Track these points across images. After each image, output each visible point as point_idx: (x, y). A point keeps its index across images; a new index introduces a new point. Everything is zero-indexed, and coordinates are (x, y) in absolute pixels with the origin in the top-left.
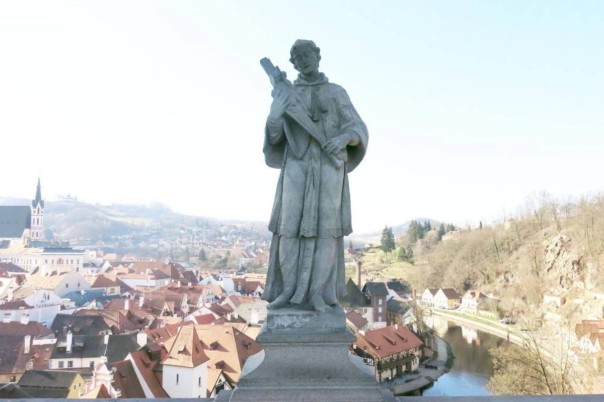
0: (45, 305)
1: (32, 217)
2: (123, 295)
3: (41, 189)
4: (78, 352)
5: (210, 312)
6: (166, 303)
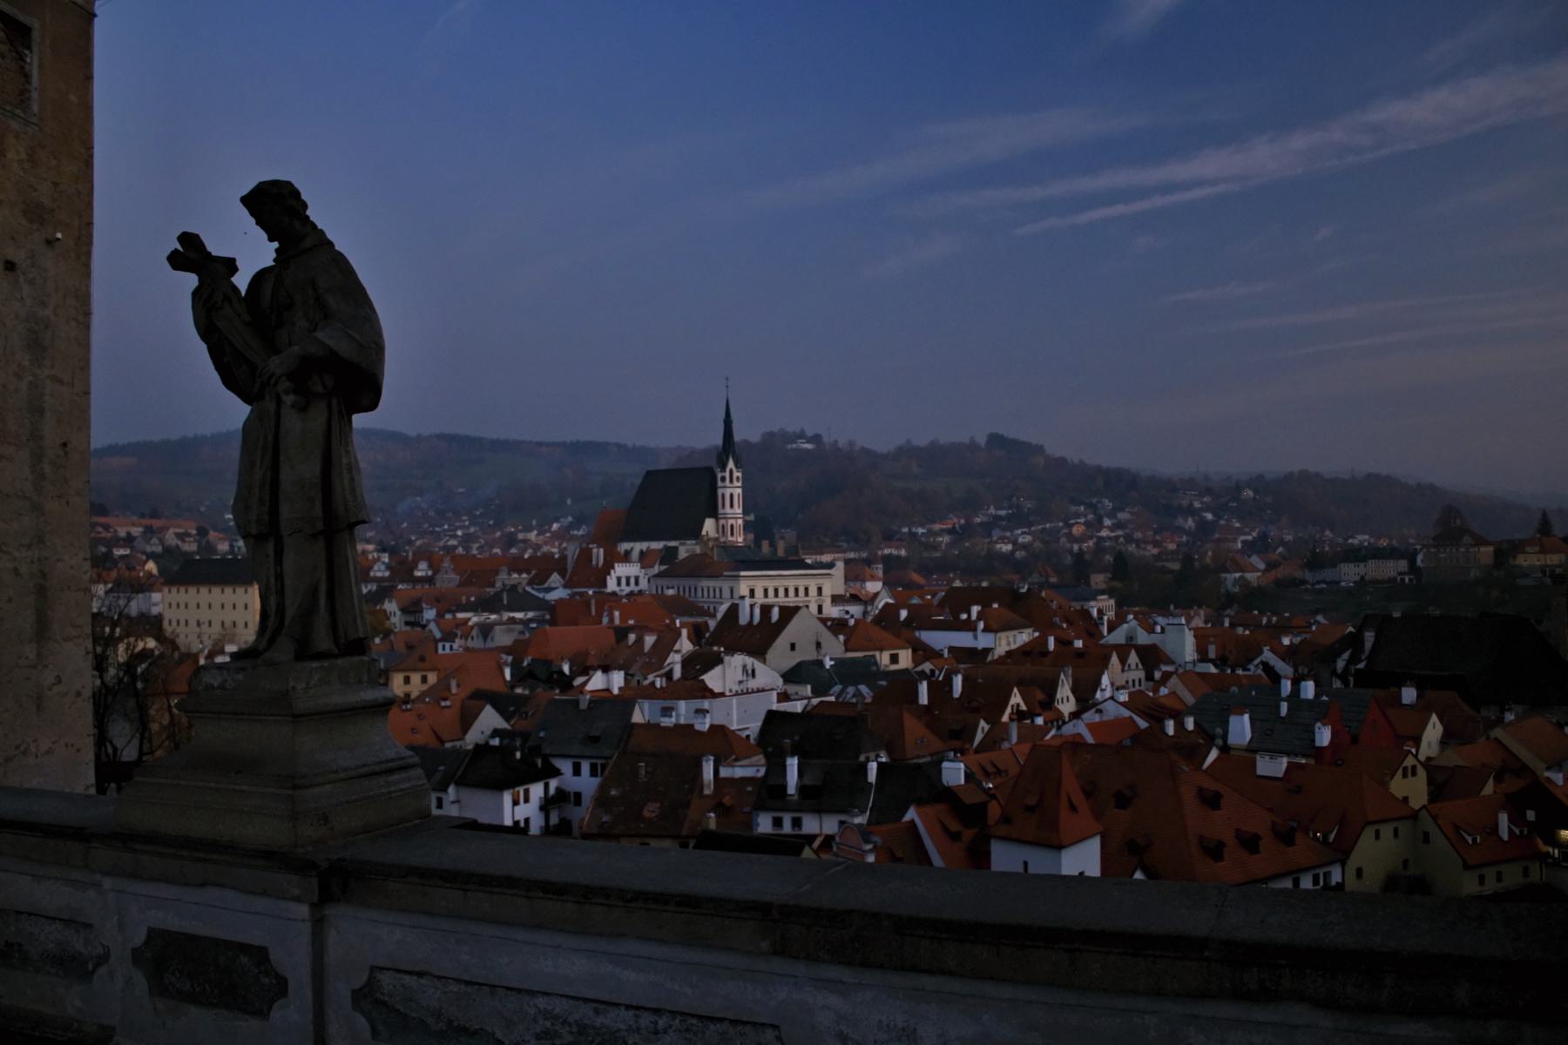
0: (747, 689)
1: (720, 492)
2: (919, 669)
4: (814, 798)
5: (1126, 713)
6: (1015, 690)
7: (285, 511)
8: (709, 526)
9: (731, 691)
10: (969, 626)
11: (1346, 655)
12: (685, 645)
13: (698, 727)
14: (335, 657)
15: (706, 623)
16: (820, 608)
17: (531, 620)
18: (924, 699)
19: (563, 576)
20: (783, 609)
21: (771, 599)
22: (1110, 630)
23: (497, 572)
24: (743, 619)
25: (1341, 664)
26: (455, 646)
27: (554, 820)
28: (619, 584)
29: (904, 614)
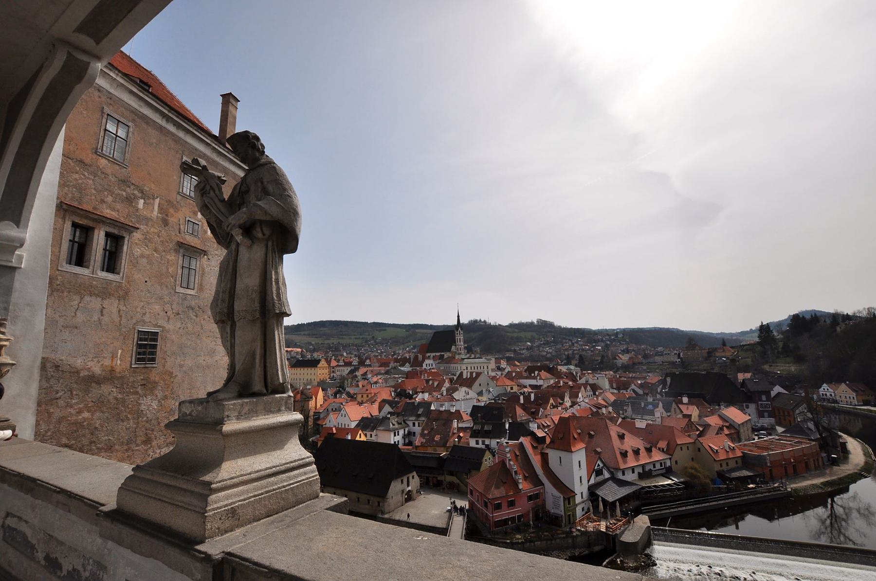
1: (456, 337)
3: (460, 318)
7: (237, 306)
8: (453, 348)
10: (535, 378)
11: (661, 387)
12: (447, 384)
13: (451, 411)
14: (264, 395)
16: (488, 372)
18: (522, 401)
19: (410, 363)
20: (477, 373)
21: (473, 370)
22: (580, 379)
23: (390, 363)
24: (464, 377)
25: (659, 390)
26: (377, 386)
27: (407, 441)
28: (427, 366)
29: (514, 374)
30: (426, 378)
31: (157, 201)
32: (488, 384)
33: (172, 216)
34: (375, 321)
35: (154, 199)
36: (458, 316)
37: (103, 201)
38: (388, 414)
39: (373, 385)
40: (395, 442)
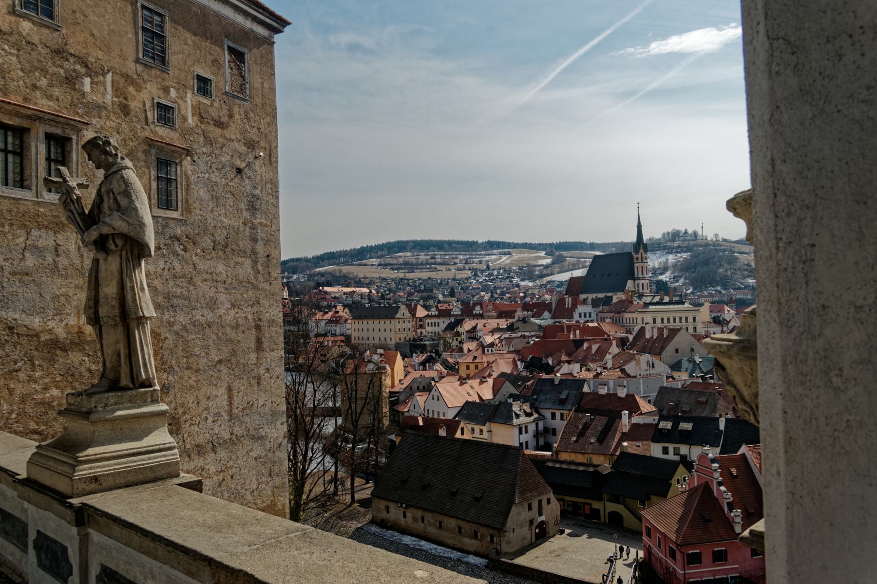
1: (636, 265)
8: (630, 284)
9: (640, 375)
13: (619, 395)
15: (627, 338)
16: (695, 328)
17: (532, 336)
19: (550, 312)
23: (516, 311)
24: (648, 336)
26: (494, 349)
27: (541, 442)
28: (580, 316)
30: (578, 337)
31: (109, 77)
32: (692, 350)
33: (134, 98)
34: (491, 240)
35: (104, 75)
36: (639, 227)
37: (35, 87)
38: (509, 397)
39: (486, 349)
40: (521, 444)
